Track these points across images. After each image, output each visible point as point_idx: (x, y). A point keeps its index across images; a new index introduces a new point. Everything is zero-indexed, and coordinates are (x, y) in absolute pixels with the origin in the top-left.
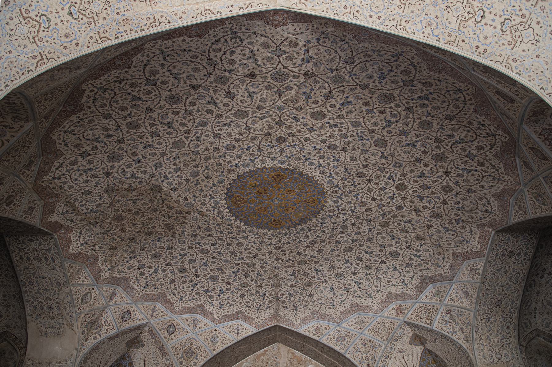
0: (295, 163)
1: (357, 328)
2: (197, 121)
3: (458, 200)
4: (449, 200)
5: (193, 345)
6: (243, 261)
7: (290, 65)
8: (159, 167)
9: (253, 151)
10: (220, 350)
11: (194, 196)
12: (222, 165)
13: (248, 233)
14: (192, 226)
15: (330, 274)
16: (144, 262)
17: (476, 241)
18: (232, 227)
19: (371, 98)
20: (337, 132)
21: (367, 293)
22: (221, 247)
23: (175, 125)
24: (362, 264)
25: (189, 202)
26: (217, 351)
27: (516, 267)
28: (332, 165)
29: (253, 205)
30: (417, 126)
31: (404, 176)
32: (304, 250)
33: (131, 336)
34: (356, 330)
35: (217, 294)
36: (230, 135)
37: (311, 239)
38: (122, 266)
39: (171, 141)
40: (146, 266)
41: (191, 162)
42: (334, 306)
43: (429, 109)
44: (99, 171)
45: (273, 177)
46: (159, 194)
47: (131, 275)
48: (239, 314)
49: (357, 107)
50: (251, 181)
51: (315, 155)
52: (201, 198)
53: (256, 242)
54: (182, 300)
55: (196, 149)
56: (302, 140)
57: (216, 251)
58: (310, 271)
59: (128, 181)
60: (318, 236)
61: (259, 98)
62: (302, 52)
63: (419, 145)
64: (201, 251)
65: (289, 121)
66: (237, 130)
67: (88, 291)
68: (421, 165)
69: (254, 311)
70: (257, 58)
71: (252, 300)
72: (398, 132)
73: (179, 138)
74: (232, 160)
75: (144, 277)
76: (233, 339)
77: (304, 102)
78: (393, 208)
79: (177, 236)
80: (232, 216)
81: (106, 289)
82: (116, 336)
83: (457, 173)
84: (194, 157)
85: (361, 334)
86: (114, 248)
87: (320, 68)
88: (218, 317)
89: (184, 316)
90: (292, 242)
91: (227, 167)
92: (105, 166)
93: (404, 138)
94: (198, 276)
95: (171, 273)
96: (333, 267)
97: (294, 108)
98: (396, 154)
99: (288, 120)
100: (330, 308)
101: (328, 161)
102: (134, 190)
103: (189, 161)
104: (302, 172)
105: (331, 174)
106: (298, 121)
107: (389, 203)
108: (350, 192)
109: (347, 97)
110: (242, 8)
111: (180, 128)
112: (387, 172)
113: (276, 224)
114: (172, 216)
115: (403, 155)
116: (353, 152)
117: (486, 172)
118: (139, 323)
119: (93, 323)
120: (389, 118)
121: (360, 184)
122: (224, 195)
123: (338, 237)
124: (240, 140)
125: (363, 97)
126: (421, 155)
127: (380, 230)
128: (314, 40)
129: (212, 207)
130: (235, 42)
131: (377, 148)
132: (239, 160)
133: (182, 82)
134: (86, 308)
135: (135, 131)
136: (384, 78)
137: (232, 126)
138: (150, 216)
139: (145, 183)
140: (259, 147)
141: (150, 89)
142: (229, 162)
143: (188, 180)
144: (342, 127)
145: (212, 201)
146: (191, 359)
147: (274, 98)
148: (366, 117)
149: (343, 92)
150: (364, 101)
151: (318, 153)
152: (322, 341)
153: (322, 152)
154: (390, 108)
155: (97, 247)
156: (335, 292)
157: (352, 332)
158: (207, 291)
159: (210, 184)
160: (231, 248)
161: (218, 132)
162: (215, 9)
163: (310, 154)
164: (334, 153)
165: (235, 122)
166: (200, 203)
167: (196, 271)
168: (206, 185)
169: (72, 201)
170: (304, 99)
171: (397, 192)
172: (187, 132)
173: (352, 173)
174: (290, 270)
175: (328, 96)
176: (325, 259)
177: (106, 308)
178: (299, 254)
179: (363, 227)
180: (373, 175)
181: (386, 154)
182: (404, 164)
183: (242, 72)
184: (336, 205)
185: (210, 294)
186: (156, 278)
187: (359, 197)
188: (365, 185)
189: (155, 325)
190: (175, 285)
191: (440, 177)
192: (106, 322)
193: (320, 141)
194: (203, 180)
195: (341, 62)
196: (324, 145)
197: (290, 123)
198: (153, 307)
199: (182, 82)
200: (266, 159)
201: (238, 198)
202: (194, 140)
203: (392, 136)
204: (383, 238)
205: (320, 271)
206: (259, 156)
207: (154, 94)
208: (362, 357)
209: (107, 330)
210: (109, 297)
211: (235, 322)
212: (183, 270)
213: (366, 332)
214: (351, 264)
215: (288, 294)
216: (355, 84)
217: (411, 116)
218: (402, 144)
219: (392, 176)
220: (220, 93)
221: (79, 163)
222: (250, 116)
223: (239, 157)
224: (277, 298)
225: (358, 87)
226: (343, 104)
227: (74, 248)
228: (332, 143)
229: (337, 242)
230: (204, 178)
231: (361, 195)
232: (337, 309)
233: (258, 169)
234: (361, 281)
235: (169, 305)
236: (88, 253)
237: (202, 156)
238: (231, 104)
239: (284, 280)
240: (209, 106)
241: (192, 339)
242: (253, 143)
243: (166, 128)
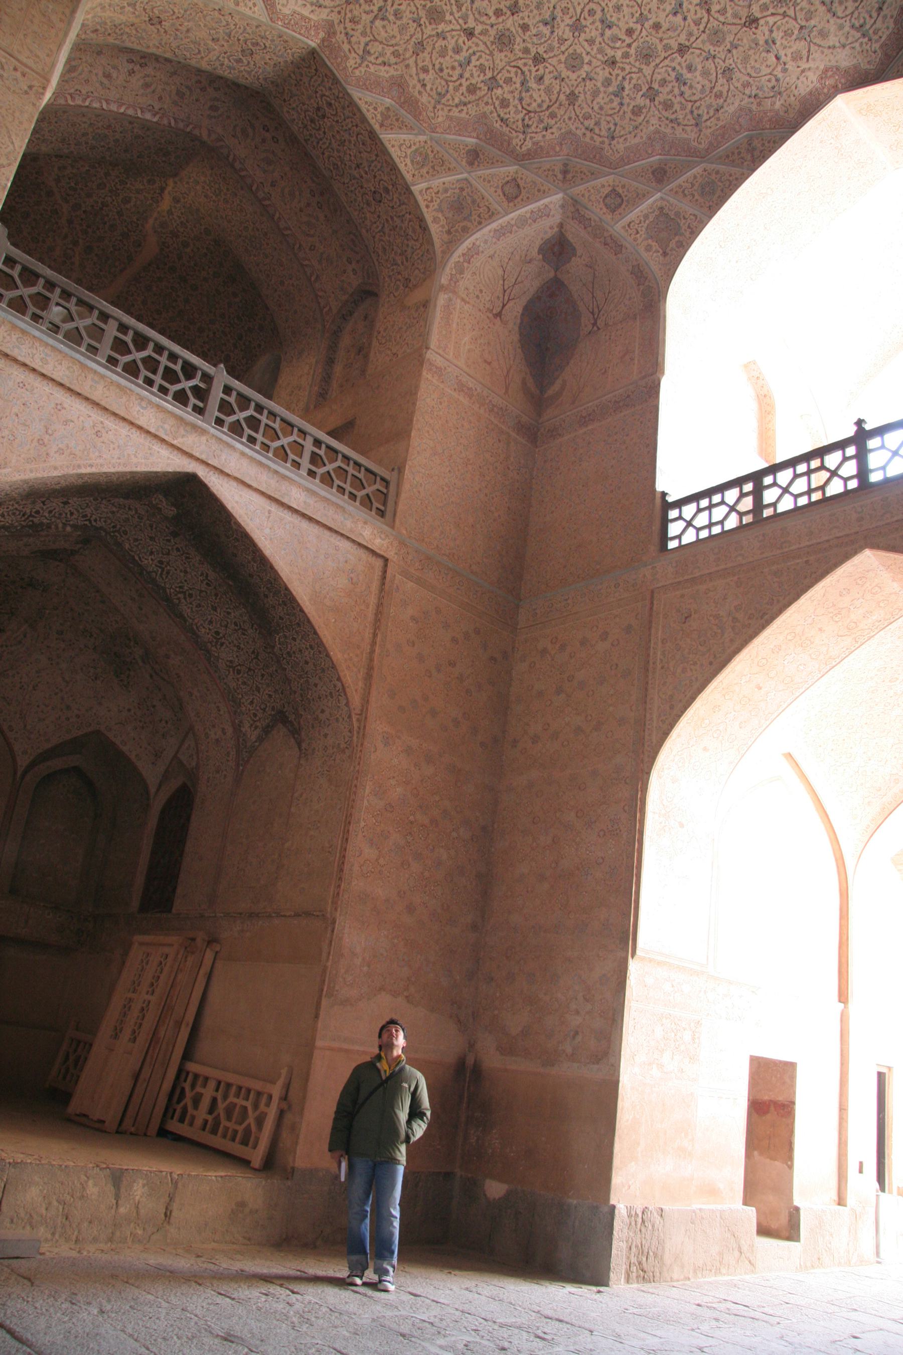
3: (405, 21)
4: (409, 5)
17: (296, 8)
19: (661, 40)
27: (216, 52)
43: (599, 84)
49: (662, 15)
62: (782, 53)
63: (546, 30)
68: (502, 6)
72: (583, 22)
83: (465, 48)
87: (748, 40)
93: (568, 21)
109: (685, 19)
117: (456, 89)
120: (615, 30)
125: (670, 33)
126: (523, 18)
128: (780, 75)
148: (636, 8)
154: (629, 46)
191: (465, 18)
195: (734, 66)
217: (599, 56)
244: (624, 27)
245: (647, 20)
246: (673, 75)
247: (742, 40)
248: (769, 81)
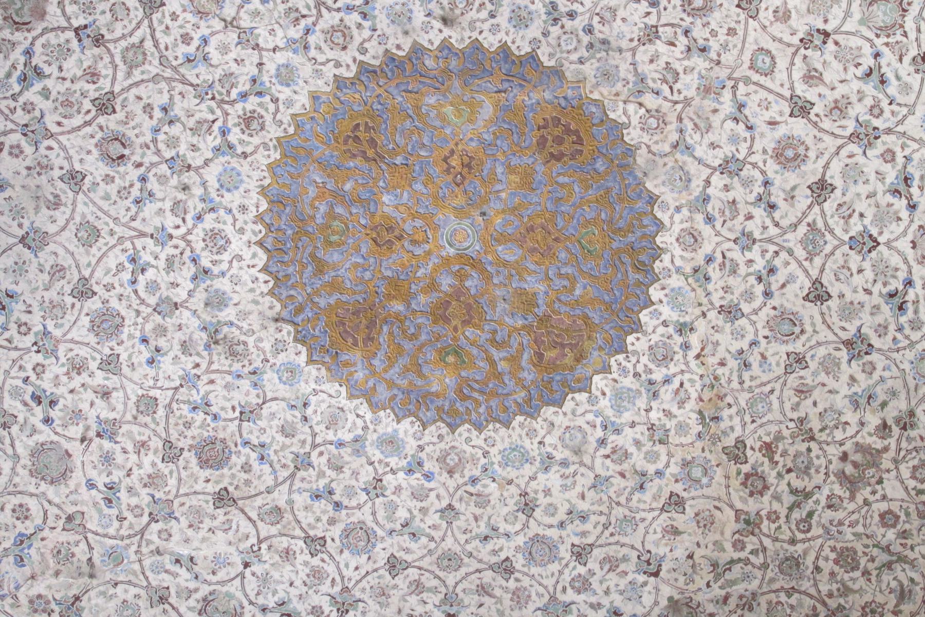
6: (888, 57)
12: (444, 503)
13: (697, 185)
14: (802, 392)
18: (709, 260)
20: (55, 369)
22: (860, 206)
29: (541, 288)
41: (498, 592)
45: (369, 339)
46: (699, 597)
50: (442, 380)
51: (180, 327)
52: (638, 460)
53: (727, 107)
57: (900, 204)
74: (405, 494)
77: (46, 533)
79: (900, 405)
84: (471, 600)
91: (443, 486)
99: (131, 509)
103: (499, 601)
104: (271, 293)
112: (28, 108)
114: (794, 492)
116: (67, 262)
121: (148, 109)
122: (568, 405)
124: (309, 540)
137: (281, 595)
138: (827, 567)
140: (293, 475)
143: (580, 554)
144: (26, 380)
147: (101, 601)
153: (149, 327)
159: (553, 479)
160: (836, 167)
163: (185, 347)
164: (120, 297)
165: (261, 601)
166: (662, 450)
170: (37, 544)
180: (77, 121)
184: (297, 60)
194: (551, 510)
201: (550, 354)
206: (325, 443)
219: (24, 79)
222: (205, 590)
223: (376, 487)
228: (92, 339)
230: (538, 513)
231: (183, 49)
233: (375, 407)
237: (451, 580)
242: (291, 502)
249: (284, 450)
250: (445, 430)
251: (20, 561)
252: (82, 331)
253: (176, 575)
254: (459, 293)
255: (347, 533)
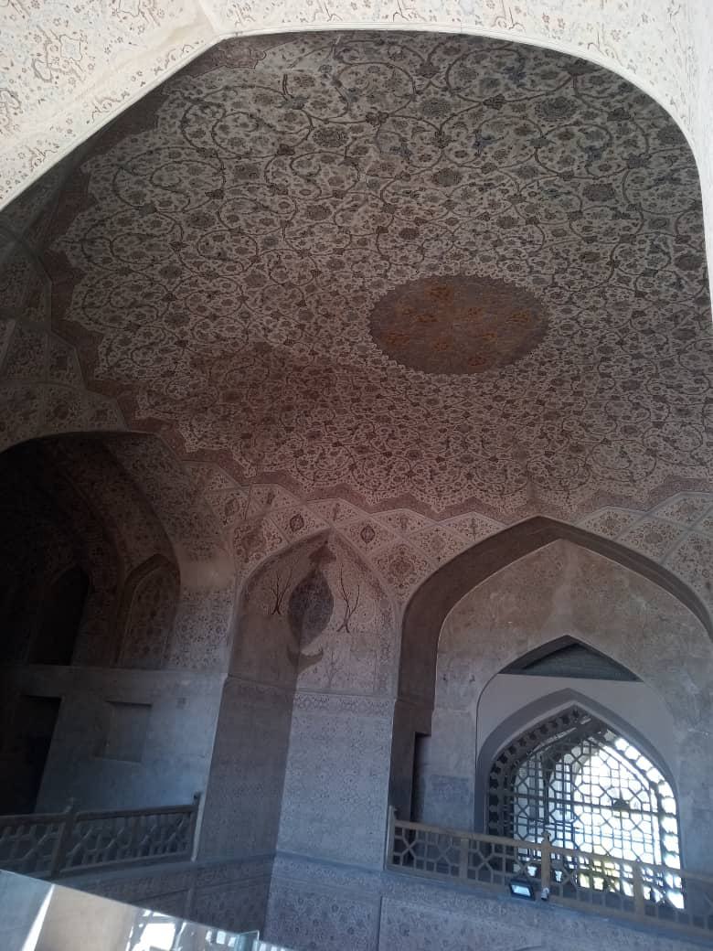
0: (456, 264)
1: (681, 519)
2: (259, 240)
5: (406, 555)
7: (327, 114)
8: (249, 317)
9: (375, 261)
10: (448, 559)
11: (324, 346)
13: (437, 384)
15: (610, 429)
16: (299, 446)
20: (499, 196)
21: (693, 457)
22: (405, 410)
23: (233, 254)
24: (669, 408)
25: (320, 355)
26: (444, 561)
28: (524, 253)
30: (657, 142)
31: (686, 242)
32: (547, 396)
33: (312, 548)
34: (683, 523)
35: (428, 477)
36: (324, 247)
37: (550, 377)
38: (269, 457)
39: (241, 277)
40: (305, 451)
42: (635, 481)
44: (168, 343)
47: (288, 467)
48: (472, 504)
51: (483, 244)
54: (376, 490)
55: (285, 281)
56: (444, 224)
58: (572, 428)
59: (216, 346)
60: (561, 371)
61: (326, 180)
64: (378, 419)
65: (402, 201)
66: (328, 237)
67: (232, 498)
69: (496, 497)
70: (269, 122)
71: (487, 480)
72: (624, 164)
73: (249, 271)
75: (308, 466)
76: (468, 542)
78: (690, 303)
80: (398, 364)
81: (261, 490)
82: (289, 551)
85: (690, 530)
86: (247, 436)
88: (439, 510)
89: (385, 514)
90: (520, 387)
92: (171, 335)
93: (644, 172)
94: (389, 454)
95: (347, 455)
96: (615, 418)
97: (396, 178)
98: (645, 205)
99: (397, 200)
100: (628, 485)
101: (513, 247)
102: (231, 357)
105: (531, 267)
106: (415, 196)
107: (675, 296)
108: (585, 290)
110: (159, 69)
111: (241, 257)
113: (475, 363)
115: (660, 202)
116: (552, 221)
118: (316, 531)
119: (251, 539)
121: (597, 273)
123: (602, 367)
127: (679, 345)
128: (332, 62)
129: (361, 356)
130: (214, 114)
131: (597, 203)
132: (362, 280)
133: (191, 194)
134: (234, 520)
135: (179, 279)
136: (522, 75)
139: (241, 344)
140: (380, 253)
141: (153, 219)
142: (348, 287)
143: (301, 327)
144: (504, 185)
145: (355, 348)
146: (405, 574)
149: (461, 124)
150: (514, 127)
151: (486, 238)
152: (618, 541)
153: (493, 235)
155: (223, 439)
156: (631, 458)
157: (674, 526)
158: (410, 474)
161: (302, 247)
162: (114, 93)
167: (383, 447)
168: (332, 328)
169: (153, 389)
171: (683, 274)
172: (256, 259)
173: (571, 258)
174: (536, 429)
175: (441, 140)
176: (592, 406)
177: (264, 515)
178: (541, 403)
179: (644, 346)
180: (617, 252)
181: (622, 210)
182: (673, 220)
183: (266, 151)
185: (416, 477)
186: (326, 466)
187: (608, 295)
188: (609, 273)
189: (342, 531)
190: (359, 472)
192: (269, 535)
193: (478, 218)
196: (490, 222)
197: (405, 203)
198: (334, 505)
199: (191, 194)
200: (405, 268)
202: (273, 268)
203: (615, 174)
204: (693, 358)
205: (591, 426)
207: (164, 223)
208: (696, 570)
209: (273, 545)
210: (265, 501)
211: (469, 516)
212: (362, 450)
213: (700, 527)
214: (648, 410)
215: (546, 467)
216: (475, 104)
217: (631, 126)
218: (646, 183)
220: (261, 190)
221: (133, 339)
222: (333, 211)
224: (527, 474)
225: (485, 107)
226: (477, 145)
227: (191, 445)
228: (502, 215)
229: (603, 375)
231: (610, 292)
232: (641, 486)
234: (676, 437)
235: (358, 500)
236: (214, 449)
238: (290, 202)
239: (532, 446)
240: (259, 214)
241: (403, 545)
243: (220, 262)
244: (572, 144)
245: (532, 142)
246: (525, 80)
247: (395, 102)
248: (353, 58)
249: (396, 256)
250: (375, 300)
251: (394, 149)
252: (512, 213)
253: (348, 203)
254: (435, 320)
255: (341, 262)
